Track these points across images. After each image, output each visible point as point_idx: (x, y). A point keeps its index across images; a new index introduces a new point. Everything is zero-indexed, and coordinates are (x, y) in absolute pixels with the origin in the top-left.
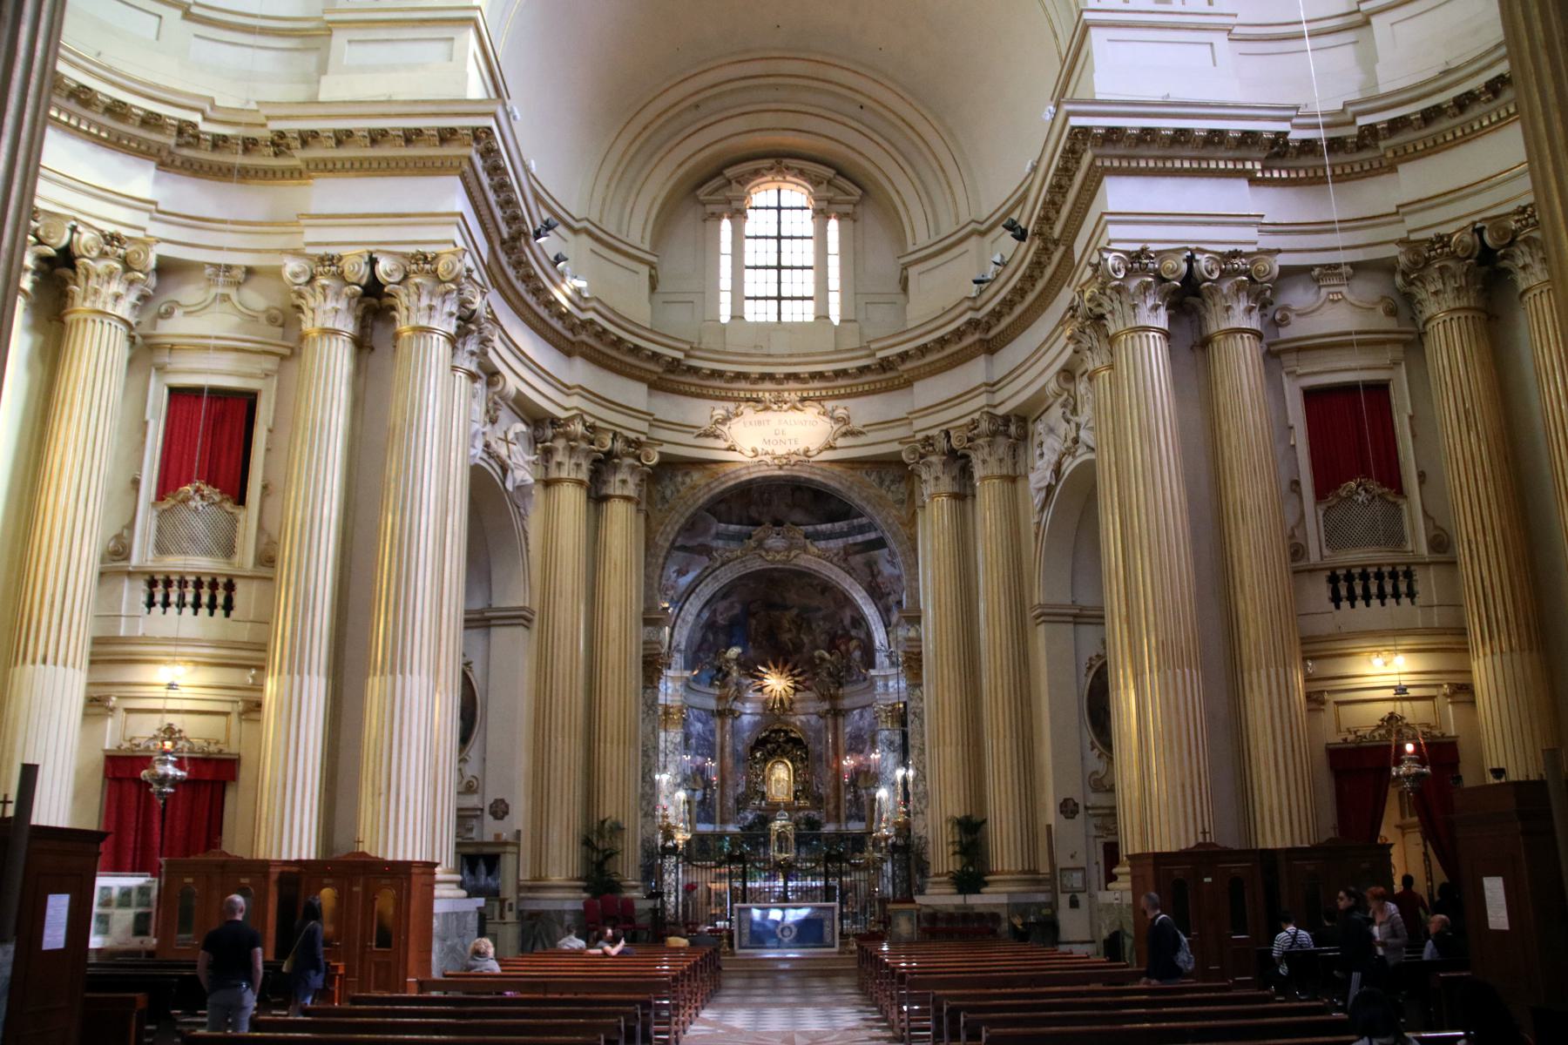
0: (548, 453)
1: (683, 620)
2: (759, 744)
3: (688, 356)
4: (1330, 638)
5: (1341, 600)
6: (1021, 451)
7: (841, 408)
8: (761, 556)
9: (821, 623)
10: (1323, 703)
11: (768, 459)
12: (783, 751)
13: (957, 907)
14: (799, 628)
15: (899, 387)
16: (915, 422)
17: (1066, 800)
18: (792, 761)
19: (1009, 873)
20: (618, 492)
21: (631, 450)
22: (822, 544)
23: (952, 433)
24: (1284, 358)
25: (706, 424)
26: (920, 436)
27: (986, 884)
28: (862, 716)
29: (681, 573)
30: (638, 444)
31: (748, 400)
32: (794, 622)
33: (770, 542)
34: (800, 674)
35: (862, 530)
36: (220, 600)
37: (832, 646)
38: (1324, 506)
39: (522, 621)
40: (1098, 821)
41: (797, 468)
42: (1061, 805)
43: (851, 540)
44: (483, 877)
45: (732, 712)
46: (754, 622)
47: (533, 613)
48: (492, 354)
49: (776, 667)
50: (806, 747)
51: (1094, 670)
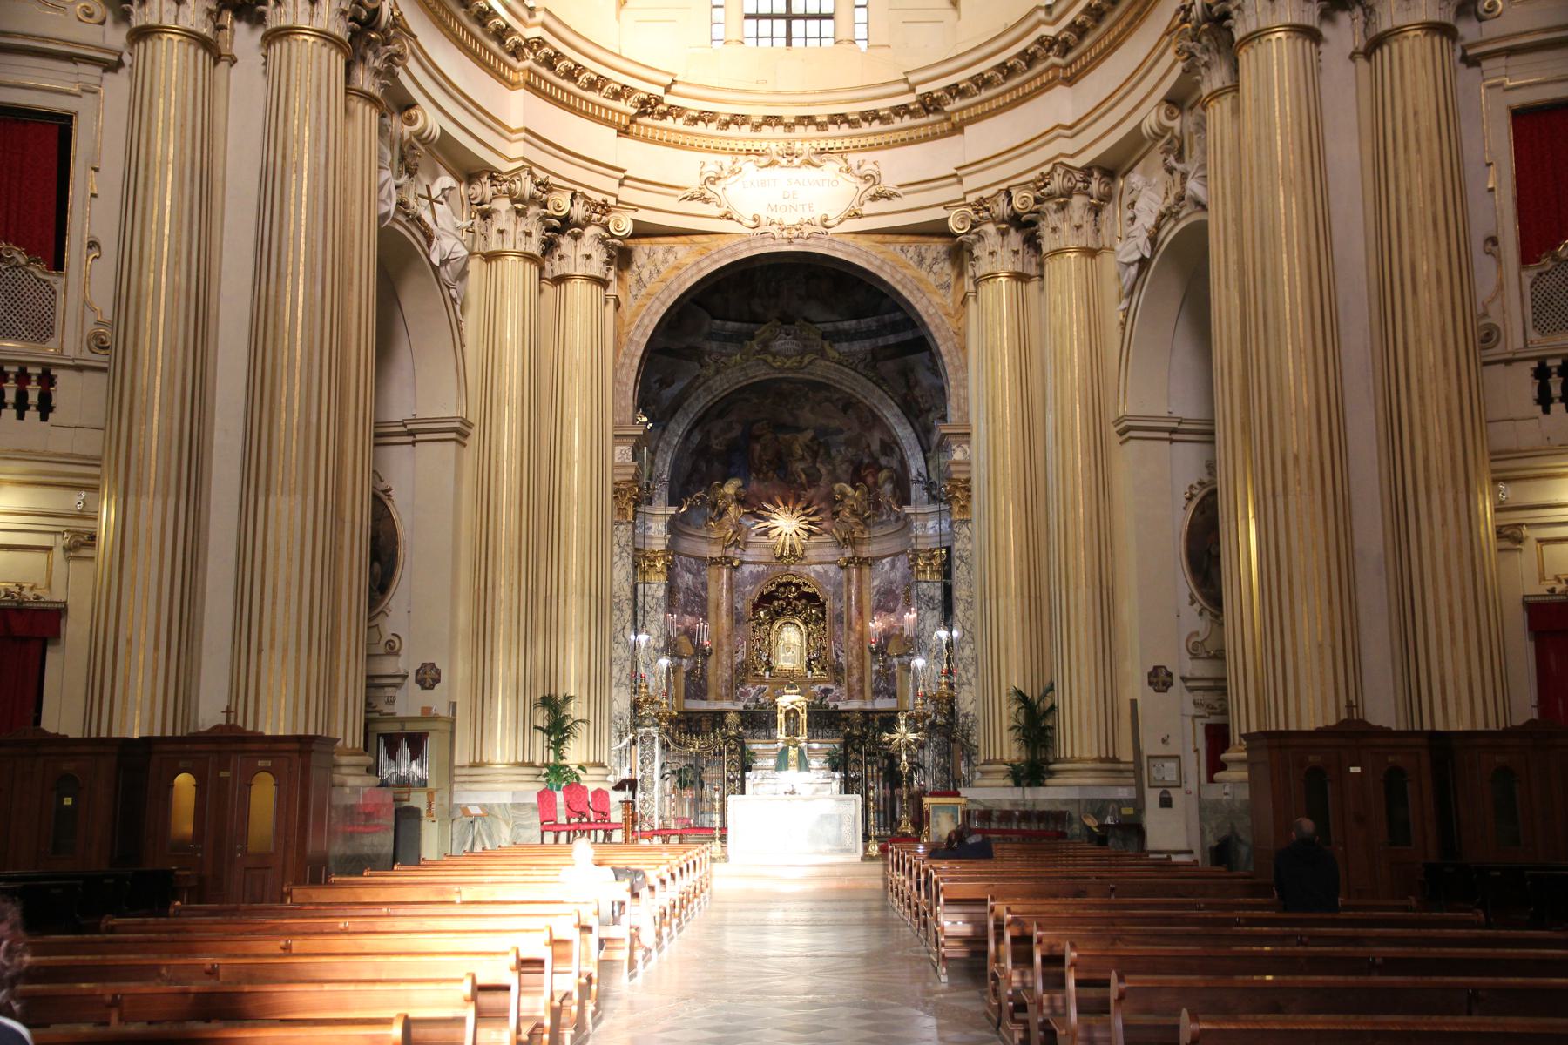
0: (486, 215)
1: (668, 444)
2: (765, 600)
3: (667, 90)
4: (1535, 453)
5: (1552, 401)
6: (1104, 215)
7: (868, 161)
8: (766, 362)
9: (842, 449)
10: (1520, 541)
11: (774, 230)
12: (794, 609)
13: (1015, 803)
15: (944, 135)
16: (965, 180)
17: (1156, 668)
18: (805, 623)
19: (1081, 760)
20: (580, 271)
21: (595, 216)
22: (845, 347)
23: (1014, 192)
24: (1485, 64)
25: (694, 183)
26: (971, 198)
27: (1052, 773)
28: (893, 566)
30: (605, 208)
31: (748, 152)
33: (777, 345)
34: (815, 514)
35: (894, 328)
36: (33, 397)
37: (856, 479)
38: (1533, 273)
39: (453, 435)
40: (1199, 696)
41: (810, 242)
42: (1150, 675)
43: (881, 342)
44: (406, 762)
45: (728, 560)
46: (758, 447)
47: (470, 426)
48: (403, 77)
49: (786, 504)
50: (823, 605)
51: (1196, 501)
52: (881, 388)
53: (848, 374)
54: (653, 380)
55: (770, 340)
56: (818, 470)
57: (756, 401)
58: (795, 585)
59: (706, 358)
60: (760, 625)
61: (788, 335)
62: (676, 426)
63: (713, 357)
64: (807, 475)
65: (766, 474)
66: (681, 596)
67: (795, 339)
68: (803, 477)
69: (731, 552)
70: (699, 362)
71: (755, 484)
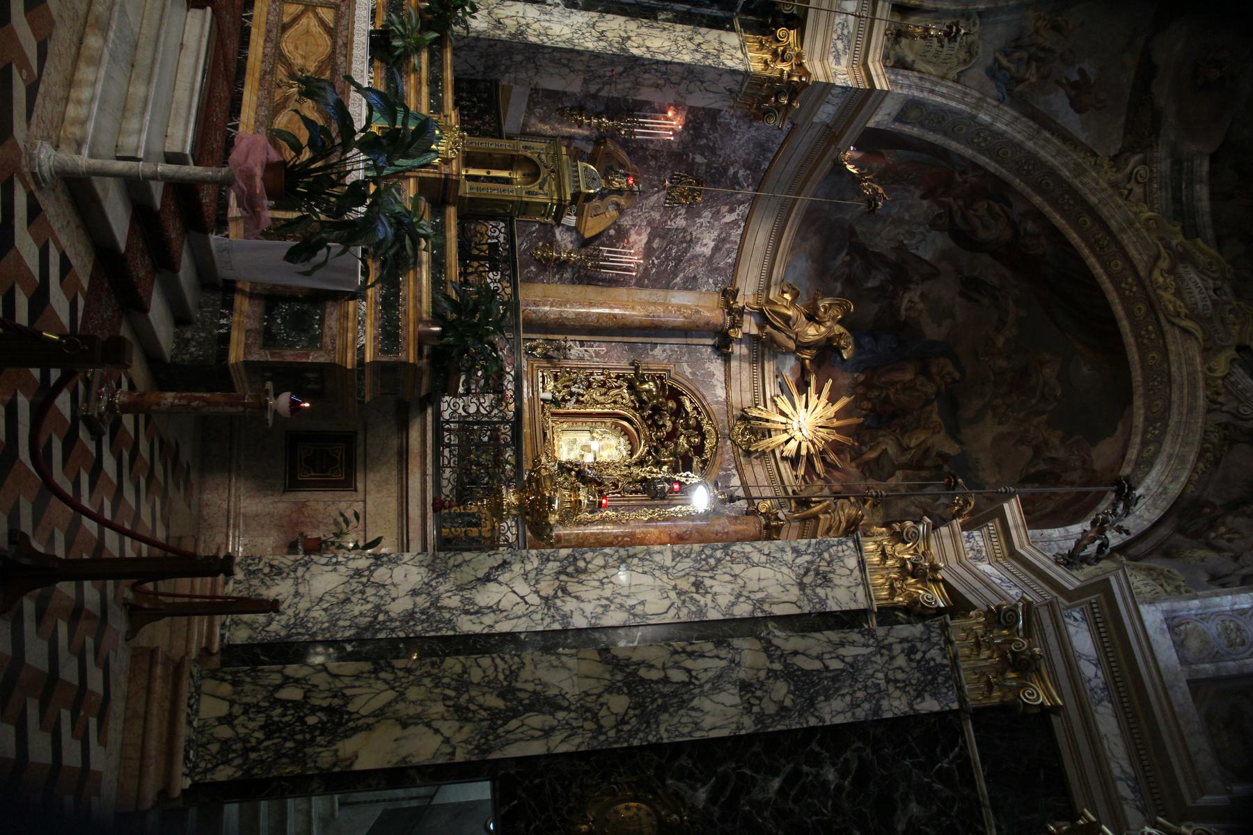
1: (977, 106)
8: (1157, 258)
14: (916, 465)
29: (1079, 95)
32: (927, 451)
33: (1192, 276)
46: (908, 376)
49: (838, 415)
52: (1198, 460)
53: (1193, 395)
54: (1085, 66)
55: (1196, 266)
56: (891, 475)
57: (1000, 342)
58: (702, 445)
59: (1138, 157)
60: (631, 387)
61: (1215, 291)
62: (1007, 117)
63: (1141, 169)
64: (877, 459)
65: (863, 397)
66: (681, 222)
67: (1215, 303)
68: (873, 455)
69: (750, 326)
70: (1121, 152)
71: (847, 382)
